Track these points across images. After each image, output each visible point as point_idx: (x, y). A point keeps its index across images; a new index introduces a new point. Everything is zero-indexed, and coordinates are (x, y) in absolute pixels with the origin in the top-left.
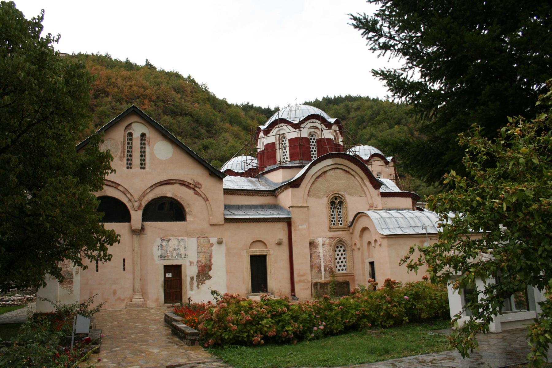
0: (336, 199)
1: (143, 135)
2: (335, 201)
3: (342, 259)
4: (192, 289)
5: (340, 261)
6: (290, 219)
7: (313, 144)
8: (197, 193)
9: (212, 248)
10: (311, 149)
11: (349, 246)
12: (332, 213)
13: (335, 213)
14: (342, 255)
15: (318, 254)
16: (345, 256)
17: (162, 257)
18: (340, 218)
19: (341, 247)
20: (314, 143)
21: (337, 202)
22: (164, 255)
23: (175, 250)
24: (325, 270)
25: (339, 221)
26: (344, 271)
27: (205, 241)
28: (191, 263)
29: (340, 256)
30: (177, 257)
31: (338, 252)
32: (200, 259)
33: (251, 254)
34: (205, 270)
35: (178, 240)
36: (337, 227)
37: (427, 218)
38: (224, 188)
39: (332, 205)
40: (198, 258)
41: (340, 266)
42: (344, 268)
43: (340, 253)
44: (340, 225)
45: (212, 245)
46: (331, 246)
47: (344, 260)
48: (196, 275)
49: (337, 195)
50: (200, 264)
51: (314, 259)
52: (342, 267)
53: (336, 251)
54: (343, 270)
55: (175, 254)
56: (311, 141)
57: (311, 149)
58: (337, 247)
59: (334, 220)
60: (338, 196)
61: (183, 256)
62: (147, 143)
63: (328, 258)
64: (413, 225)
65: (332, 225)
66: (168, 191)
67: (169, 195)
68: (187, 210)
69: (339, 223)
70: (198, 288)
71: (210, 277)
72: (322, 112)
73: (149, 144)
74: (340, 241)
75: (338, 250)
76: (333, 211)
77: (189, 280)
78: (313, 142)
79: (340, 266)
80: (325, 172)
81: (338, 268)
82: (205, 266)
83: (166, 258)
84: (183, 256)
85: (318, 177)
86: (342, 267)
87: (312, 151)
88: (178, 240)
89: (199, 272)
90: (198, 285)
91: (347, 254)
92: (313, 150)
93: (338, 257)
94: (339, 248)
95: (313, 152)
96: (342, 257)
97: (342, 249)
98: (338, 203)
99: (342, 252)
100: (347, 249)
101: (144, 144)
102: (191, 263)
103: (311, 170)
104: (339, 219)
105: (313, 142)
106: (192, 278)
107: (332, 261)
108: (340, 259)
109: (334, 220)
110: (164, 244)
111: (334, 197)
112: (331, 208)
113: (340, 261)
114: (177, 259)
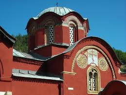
0: (93, 71)
21: (93, 73)
60: (95, 70)
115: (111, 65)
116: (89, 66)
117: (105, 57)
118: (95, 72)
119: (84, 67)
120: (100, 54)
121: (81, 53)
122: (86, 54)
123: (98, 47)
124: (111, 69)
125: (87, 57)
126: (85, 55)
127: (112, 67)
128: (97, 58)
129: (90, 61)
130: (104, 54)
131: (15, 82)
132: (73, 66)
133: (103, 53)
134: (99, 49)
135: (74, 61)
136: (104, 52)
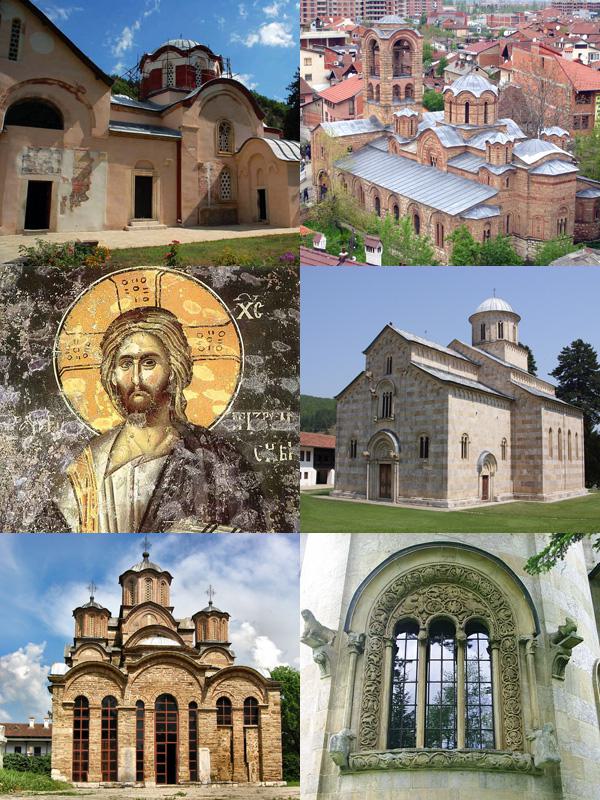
1: (16, 22)
4: (63, 212)
8: (78, 99)
17: (29, 171)
23: (45, 162)
62: (21, 30)
66: (44, 92)
67: (44, 96)
68: (65, 116)
70: (72, 210)
71: (88, 198)
73: (24, 32)
77: (60, 199)
80: (215, 97)
85: (209, 101)
90: (71, 207)
101: (18, 32)
102: (65, 179)
103: (205, 90)
106: (64, 199)
114: (46, 173)
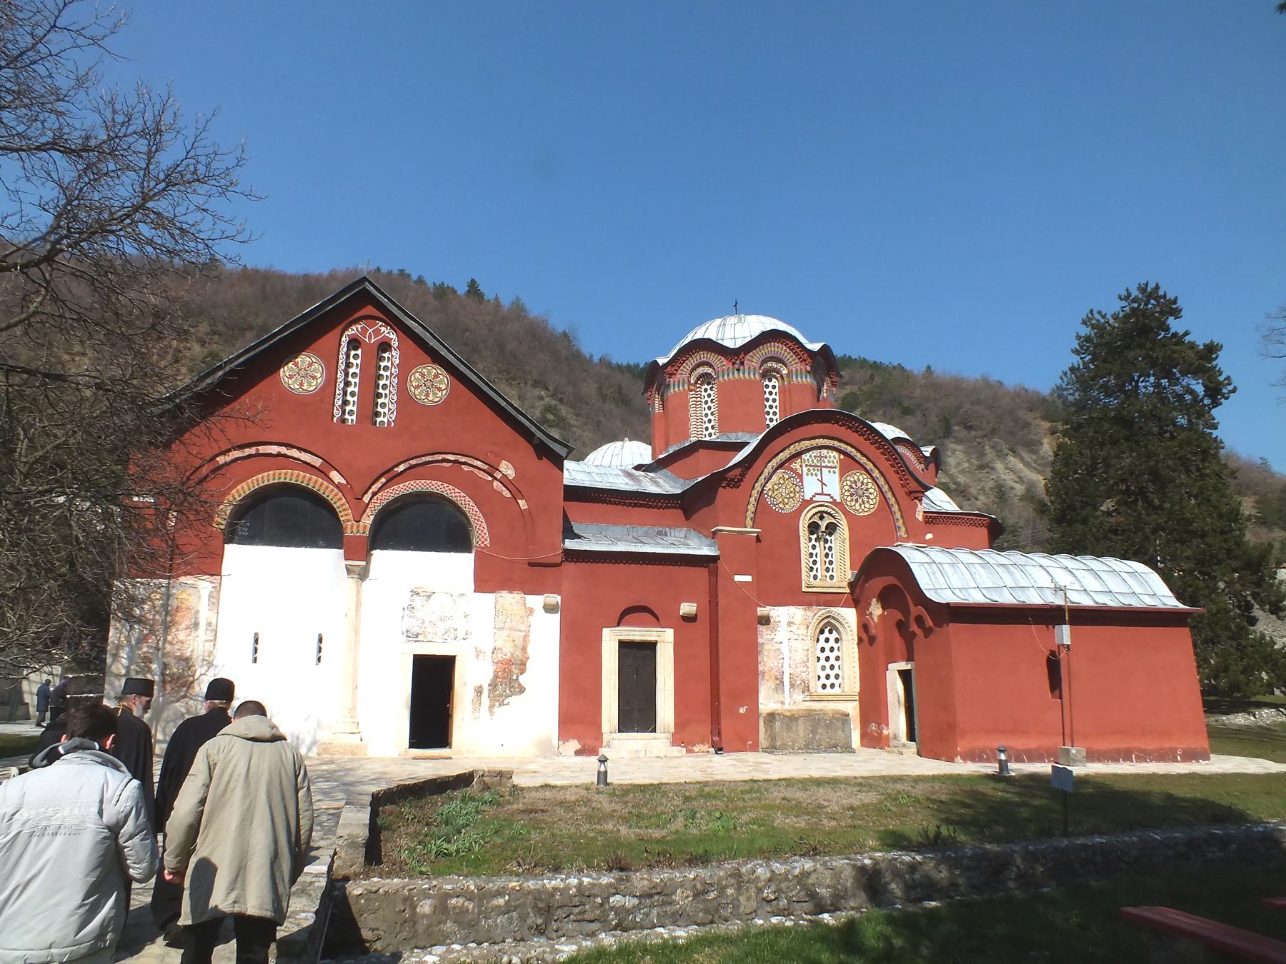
0: (822, 518)
2: (819, 522)
3: (832, 661)
5: (828, 665)
6: (714, 559)
7: (771, 398)
9: (531, 619)
10: (767, 409)
11: (848, 629)
12: (811, 550)
13: (818, 550)
14: (832, 649)
15: (778, 646)
16: (839, 654)
17: (413, 637)
18: (831, 563)
19: (830, 632)
20: (773, 396)
21: (823, 525)
22: (415, 630)
24: (792, 685)
25: (827, 570)
26: (837, 690)
27: (514, 601)
28: (478, 653)
29: (827, 653)
30: (445, 637)
31: (822, 643)
32: (499, 645)
33: (622, 638)
34: (510, 671)
35: (452, 596)
36: (822, 584)
37: (1040, 568)
38: (566, 482)
39: (812, 533)
40: (495, 641)
41: (828, 677)
42: (837, 683)
43: (827, 646)
44: (828, 579)
45: (531, 611)
46: (808, 627)
47: (836, 664)
48: (489, 682)
49: (826, 509)
50: (499, 656)
51: (768, 656)
52: (832, 680)
53: (818, 640)
54: (833, 686)
55: (442, 627)
56: (767, 391)
57: (767, 409)
58: (822, 632)
59: (815, 567)
60: (826, 513)
61: (461, 634)
63: (800, 656)
64: (1010, 583)
65: (812, 579)
69: (828, 575)
71: (522, 690)
72: (793, 329)
74: (829, 617)
75: (822, 638)
76: (814, 547)
77: (472, 694)
78: (771, 393)
79: (828, 677)
81: (823, 680)
82: (510, 662)
83: (420, 638)
84: (461, 634)
86: (832, 680)
87: (768, 400)
88: (452, 596)
89: (496, 677)
90: (491, 707)
91: (844, 648)
92: (771, 411)
93: (823, 656)
94: (826, 634)
95: (771, 416)
96: (833, 656)
97: (835, 635)
98: (827, 527)
99: (832, 643)
100: (844, 637)
104: (827, 565)
105: (771, 393)
106: (479, 691)
107: (808, 664)
108: (827, 659)
109: (815, 567)
110: (418, 602)
111: (816, 513)
112: (810, 540)
113: (828, 665)
115: (889, 495)
116: (806, 503)
117: (866, 470)
118: (828, 520)
119: (790, 507)
120: (848, 465)
121: (780, 466)
122: (796, 465)
123: (840, 441)
124: (890, 507)
125: (800, 476)
126: (795, 471)
127: (892, 501)
128: (837, 475)
129: (811, 487)
130: (863, 460)
131: (570, 568)
132: (751, 508)
133: (858, 456)
134: (843, 446)
135: (755, 493)
136: (863, 455)
